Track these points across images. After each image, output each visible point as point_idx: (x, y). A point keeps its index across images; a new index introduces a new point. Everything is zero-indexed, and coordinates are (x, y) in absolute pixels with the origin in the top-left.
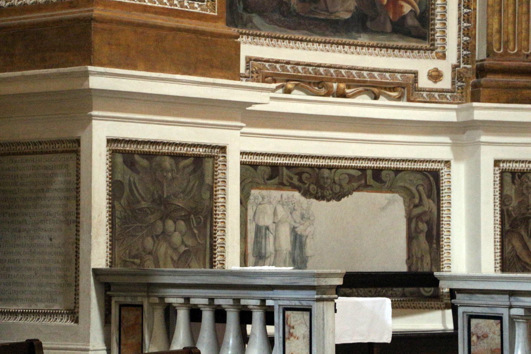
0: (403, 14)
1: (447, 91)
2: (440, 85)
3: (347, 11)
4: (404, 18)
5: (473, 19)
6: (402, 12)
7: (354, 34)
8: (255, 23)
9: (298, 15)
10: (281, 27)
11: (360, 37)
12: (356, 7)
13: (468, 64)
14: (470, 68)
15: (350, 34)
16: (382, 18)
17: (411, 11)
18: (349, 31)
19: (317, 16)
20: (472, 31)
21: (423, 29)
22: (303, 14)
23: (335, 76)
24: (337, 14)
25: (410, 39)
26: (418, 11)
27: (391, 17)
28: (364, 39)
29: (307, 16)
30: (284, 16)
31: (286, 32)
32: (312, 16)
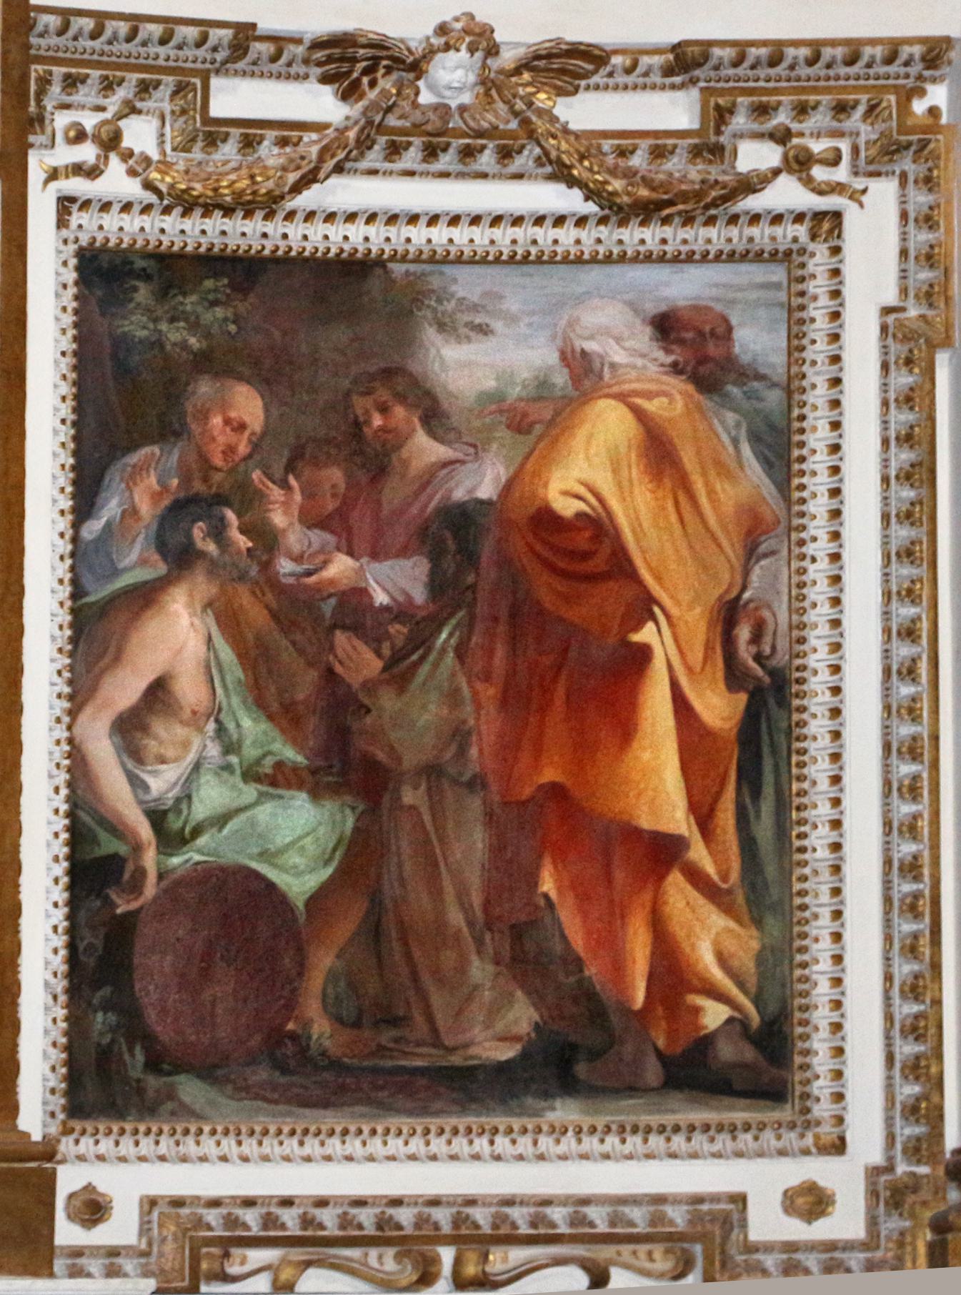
0: (703, 1033)
1: (849, 1246)
2: (822, 1230)
3: (505, 1038)
4: (706, 1042)
5: (932, 1031)
6: (698, 1027)
7: (529, 1101)
8: (187, 1099)
9: (335, 1065)
10: (276, 1102)
11: (553, 1109)
12: (537, 1023)
13: (919, 1162)
14: (927, 1176)
15: (514, 1103)
16: (628, 1049)
17: (730, 1021)
18: (514, 1096)
19: (403, 1063)
20: (928, 1067)
21: (774, 1071)
22: (355, 1061)
23: (446, 1229)
24: (473, 1051)
25: (727, 1101)
26: (755, 1019)
27: (661, 1043)
28: (565, 1111)
29: (366, 1063)
30: (285, 1070)
31: (289, 1114)
32: (389, 1063)
